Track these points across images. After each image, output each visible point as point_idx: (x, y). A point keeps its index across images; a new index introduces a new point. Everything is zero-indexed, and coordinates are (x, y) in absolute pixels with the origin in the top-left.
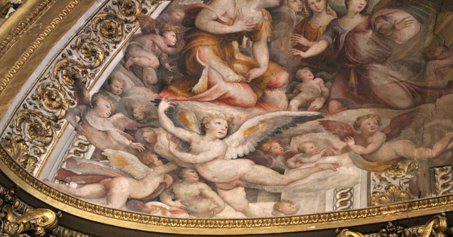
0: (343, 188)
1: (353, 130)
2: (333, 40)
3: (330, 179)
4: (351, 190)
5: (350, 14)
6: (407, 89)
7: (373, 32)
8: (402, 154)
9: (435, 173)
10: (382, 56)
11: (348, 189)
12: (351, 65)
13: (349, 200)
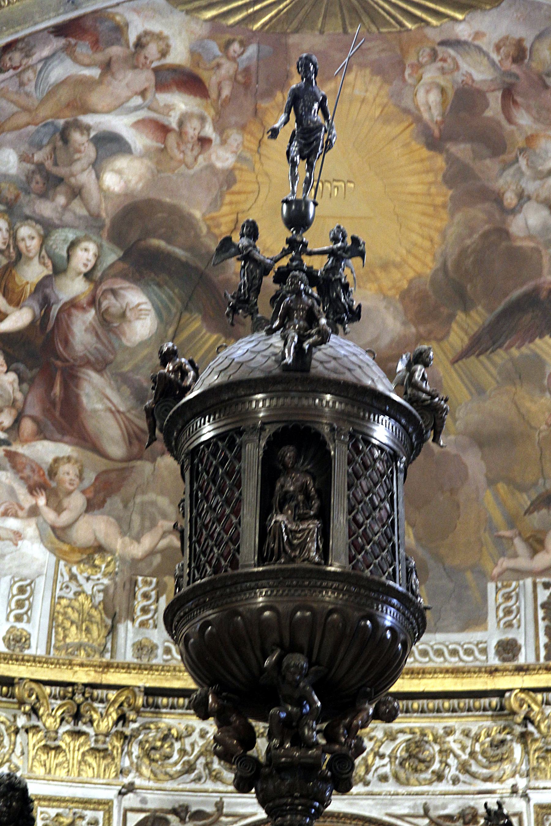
0: (23, 577)
1: (47, 477)
2: (41, 311)
3: (8, 557)
4: (32, 582)
5: (71, 273)
6: (124, 429)
7: (96, 312)
8: (103, 541)
9: (136, 583)
10: (100, 359)
11: (28, 581)
12: (59, 363)
13: (28, 599)
